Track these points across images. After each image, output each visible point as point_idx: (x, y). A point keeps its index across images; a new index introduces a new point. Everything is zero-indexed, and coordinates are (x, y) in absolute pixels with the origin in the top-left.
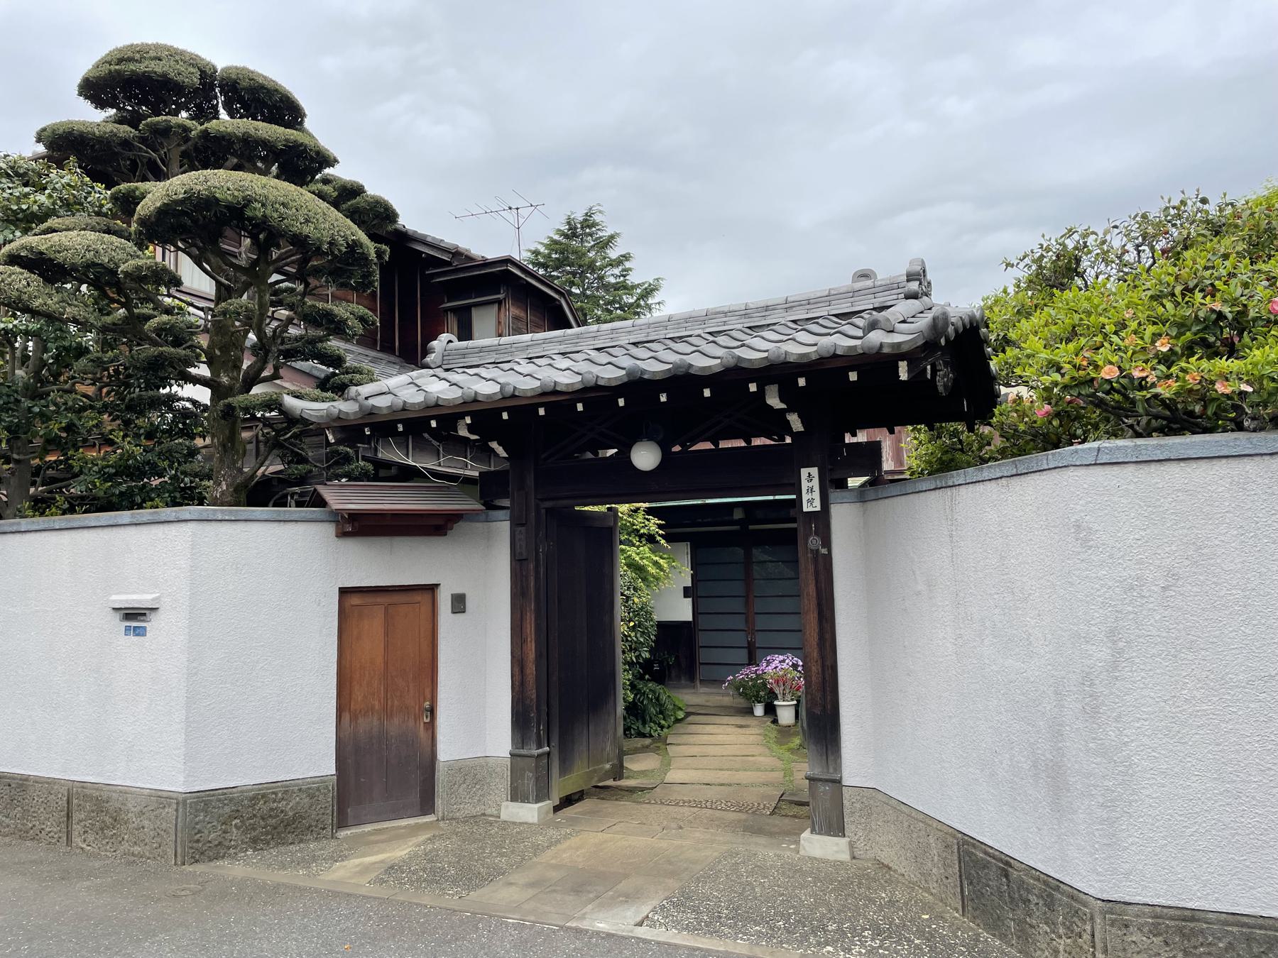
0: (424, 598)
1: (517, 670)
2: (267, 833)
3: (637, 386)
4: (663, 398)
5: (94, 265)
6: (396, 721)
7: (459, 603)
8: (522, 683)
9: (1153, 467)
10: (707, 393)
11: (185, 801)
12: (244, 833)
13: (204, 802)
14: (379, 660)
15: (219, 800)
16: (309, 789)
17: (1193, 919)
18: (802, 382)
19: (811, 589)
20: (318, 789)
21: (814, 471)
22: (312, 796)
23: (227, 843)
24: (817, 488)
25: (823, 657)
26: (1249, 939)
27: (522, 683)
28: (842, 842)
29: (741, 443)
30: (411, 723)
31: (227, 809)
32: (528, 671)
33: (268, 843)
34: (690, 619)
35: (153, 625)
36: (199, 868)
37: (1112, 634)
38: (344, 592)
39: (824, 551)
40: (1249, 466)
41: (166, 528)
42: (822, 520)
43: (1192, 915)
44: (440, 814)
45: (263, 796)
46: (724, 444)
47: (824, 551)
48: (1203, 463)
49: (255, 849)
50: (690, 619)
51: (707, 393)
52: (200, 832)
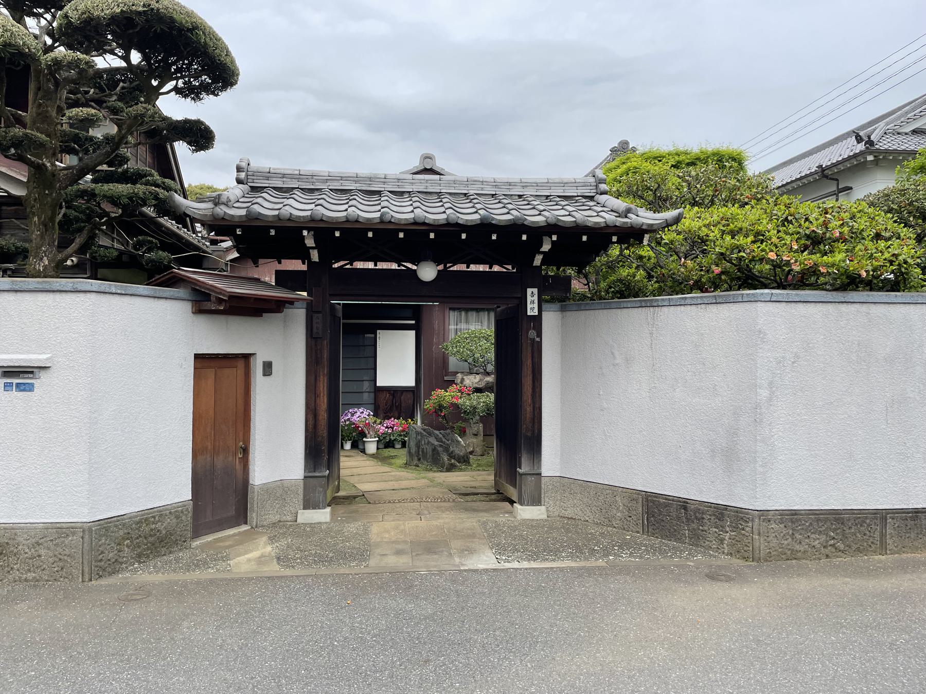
0: (241, 364)
1: (311, 417)
2: (148, 549)
3: (485, 227)
4: (494, 237)
5: (10, 45)
6: (221, 457)
7: (268, 368)
8: (315, 426)
9: (793, 304)
10: (524, 237)
11: (90, 529)
12: (133, 550)
13: (106, 527)
14: (211, 412)
15: (116, 526)
16: (174, 512)
17: (796, 514)
18: (585, 238)
19: (529, 362)
20: (182, 512)
21: (535, 290)
22: (177, 517)
23: (120, 560)
24: (536, 301)
25: (534, 402)
26: (818, 520)
27: (315, 426)
28: (543, 508)
29: (394, 266)
30: (230, 459)
31: (121, 533)
32: (321, 418)
33: (148, 557)
34: (413, 384)
35: (41, 383)
36: (103, 582)
37: (771, 383)
38: (197, 356)
39: (538, 339)
40: (830, 307)
41: (58, 296)
42: (537, 321)
43: (794, 513)
44: (255, 523)
45: (146, 520)
46: (473, 268)
47: (538, 339)
48: (813, 304)
49: (140, 563)
50: (413, 384)
51: (524, 237)
52: (102, 552)
